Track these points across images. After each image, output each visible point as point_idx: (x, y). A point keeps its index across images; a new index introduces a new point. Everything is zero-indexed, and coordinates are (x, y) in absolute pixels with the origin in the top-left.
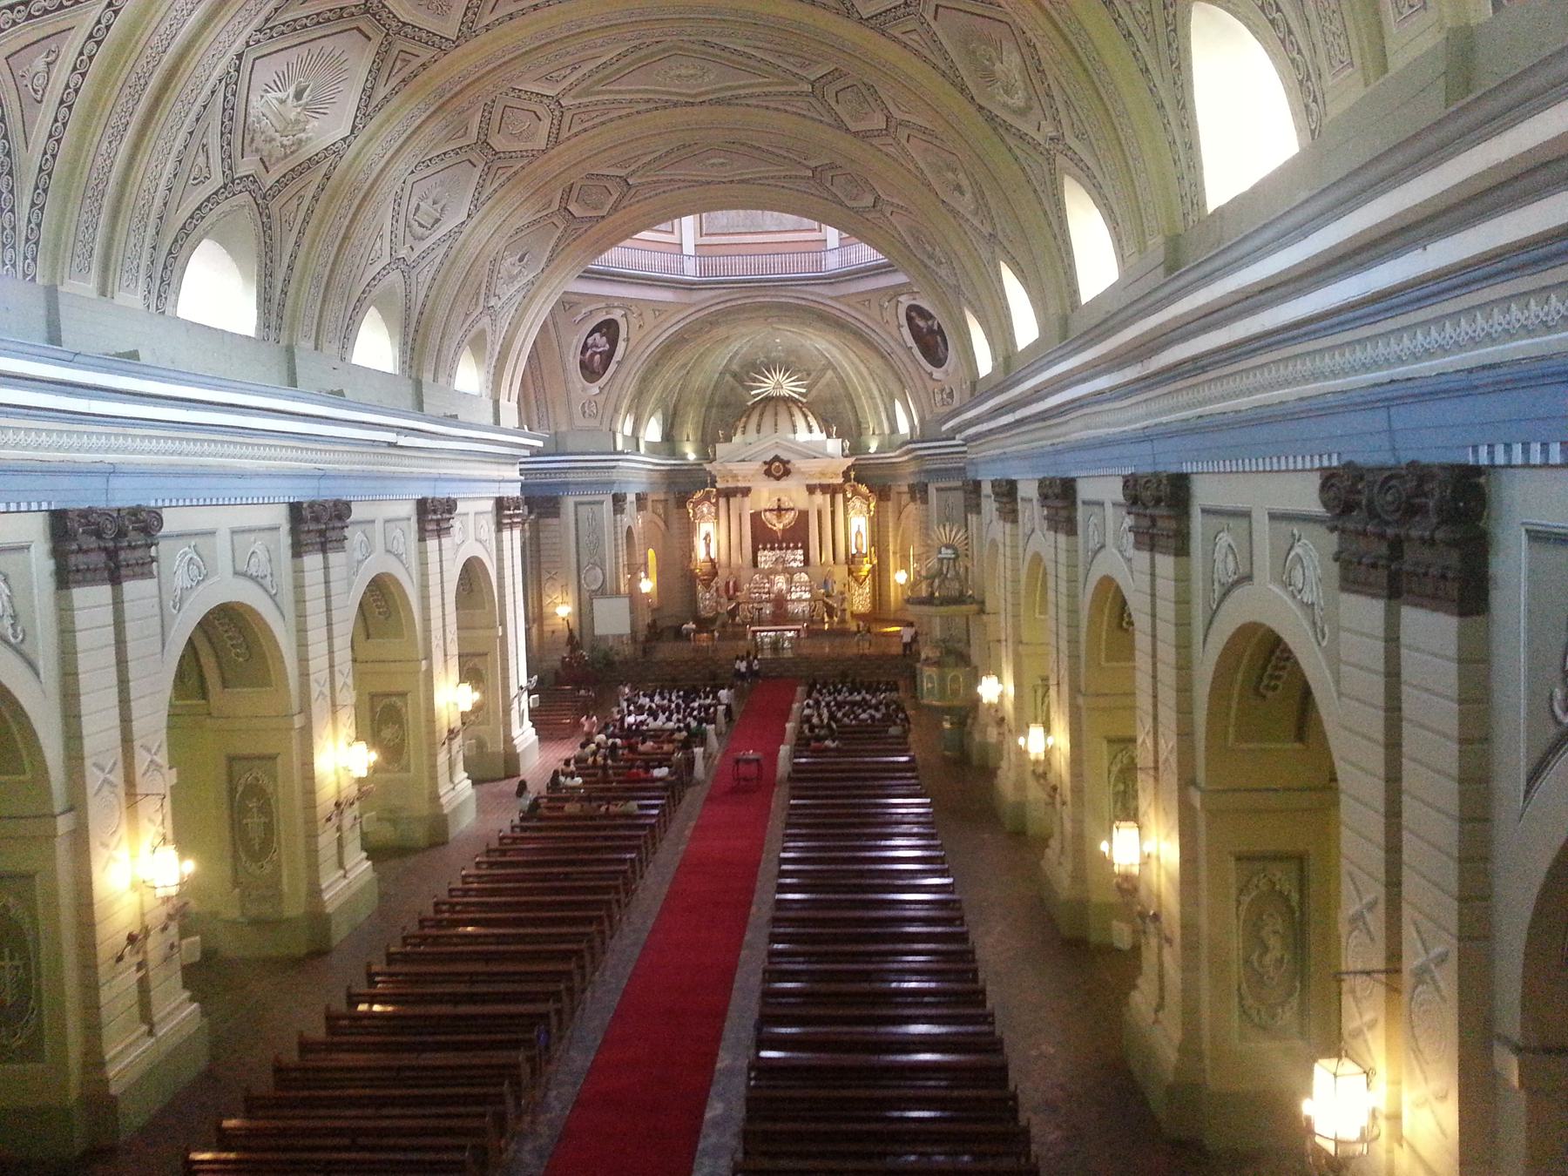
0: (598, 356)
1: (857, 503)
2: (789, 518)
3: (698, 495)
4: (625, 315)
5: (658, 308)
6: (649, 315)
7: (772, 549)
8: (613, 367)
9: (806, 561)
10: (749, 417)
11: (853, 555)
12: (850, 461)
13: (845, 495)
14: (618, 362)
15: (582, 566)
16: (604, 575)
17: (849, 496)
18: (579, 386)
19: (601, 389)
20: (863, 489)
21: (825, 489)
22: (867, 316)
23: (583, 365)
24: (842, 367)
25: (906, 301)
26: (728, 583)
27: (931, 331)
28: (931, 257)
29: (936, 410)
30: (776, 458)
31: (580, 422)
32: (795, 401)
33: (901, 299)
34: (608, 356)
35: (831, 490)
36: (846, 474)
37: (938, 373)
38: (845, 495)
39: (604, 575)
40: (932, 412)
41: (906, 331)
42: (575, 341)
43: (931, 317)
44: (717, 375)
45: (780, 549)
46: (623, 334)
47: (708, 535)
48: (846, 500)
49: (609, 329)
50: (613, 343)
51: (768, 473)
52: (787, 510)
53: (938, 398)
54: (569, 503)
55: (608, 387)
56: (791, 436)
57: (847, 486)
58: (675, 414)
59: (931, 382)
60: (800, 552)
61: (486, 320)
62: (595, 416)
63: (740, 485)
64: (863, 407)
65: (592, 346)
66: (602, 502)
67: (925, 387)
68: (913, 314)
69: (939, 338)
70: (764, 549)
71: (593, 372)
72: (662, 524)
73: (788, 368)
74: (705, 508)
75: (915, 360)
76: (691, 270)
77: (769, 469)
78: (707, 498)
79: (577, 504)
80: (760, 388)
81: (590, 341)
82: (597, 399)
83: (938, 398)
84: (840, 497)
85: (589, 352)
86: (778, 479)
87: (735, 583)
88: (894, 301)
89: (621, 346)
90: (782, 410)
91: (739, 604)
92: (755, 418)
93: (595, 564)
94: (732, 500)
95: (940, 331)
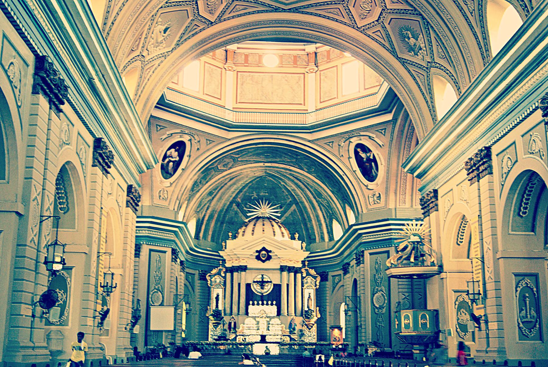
0: (171, 164)
1: (309, 279)
2: (269, 288)
3: (214, 271)
4: (190, 140)
5: (211, 139)
6: (203, 141)
7: (258, 304)
8: (179, 171)
9: (279, 313)
10: (246, 226)
11: (306, 311)
12: (307, 254)
13: (302, 275)
14: (183, 169)
15: (151, 290)
16: (163, 297)
17: (304, 275)
18: (159, 179)
19: (171, 184)
20: (312, 272)
21: (290, 269)
22: (329, 151)
23: (163, 167)
24: (302, 203)
25: (355, 141)
26: (230, 323)
27: (368, 159)
28: (411, 49)
29: (370, 207)
30: (264, 249)
31: (157, 201)
32: (274, 220)
33: (351, 140)
34: (177, 165)
35: (296, 271)
36: (303, 262)
37: (371, 185)
38: (302, 275)
39: (163, 297)
40: (367, 208)
41: (353, 161)
42: (160, 151)
43: (370, 151)
44: (229, 203)
45: (263, 304)
46: (187, 152)
47: (218, 296)
48: (303, 278)
49: (180, 147)
50: (181, 156)
51: (258, 258)
52: (267, 282)
53: (371, 200)
54: (145, 249)
55: (174, 184)
56: (273, 237)
57: (303, 270)
59: (367, 190)
61: (138, 63)
62: (166, 199)
65: (169, 157)
66: (165, 252)
67: (363, 194)
68: (359, 150)
69: (373, 164)
70: (253, 304)
71: (167, 172)
73: (270, 202)
75: (357, 178)
76: (230, 117)
77: (259, 255)
78: (219, 274)
79: (151, 250)
80: (253, 212)
81: (168, 153)
82: (167, 189)
83: (371, 200)
84: (299, 276)
85: (167, 160)
87: (235, 323)
88: (347, 142)
89: (185, 159)
90: (267, 222)
91: (237, 336)
92: (251, 226)
93: (158, 290)
95: (374, 160)
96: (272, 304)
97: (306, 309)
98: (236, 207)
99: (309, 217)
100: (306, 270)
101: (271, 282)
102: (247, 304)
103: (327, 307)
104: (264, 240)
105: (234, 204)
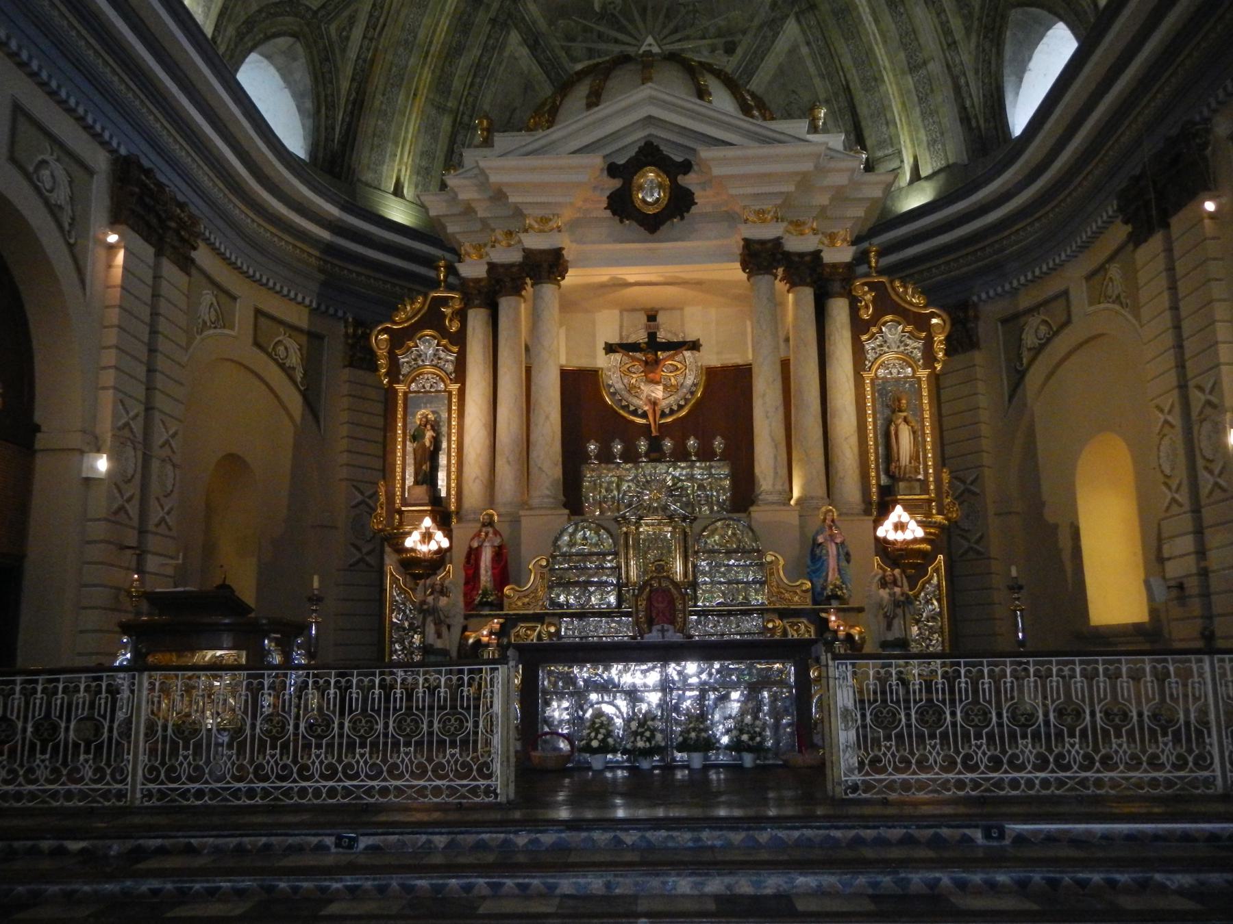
1: (892, 331)
7: (630, 456)
48: (859, 327)
56: (694, 104)
58: (358, 105)
60: (722, 471)
63: (535, 242)
64: (882, 112)
70: (606, 457)
72: (295, 402)
74: (427, 346)
78: (432, 319)
84: (839, 310)
86: (652, 224)
87: (499, 555)
94: (505, 303)
96: (706, 454)
97: (884, 480)
98: (525, 51)
99: (866, 59)
100: (872, 286)
101: (695, 346)
102: (573, 459)
103: (987, 472)
104: (650, 120)
105: (514, 37)
